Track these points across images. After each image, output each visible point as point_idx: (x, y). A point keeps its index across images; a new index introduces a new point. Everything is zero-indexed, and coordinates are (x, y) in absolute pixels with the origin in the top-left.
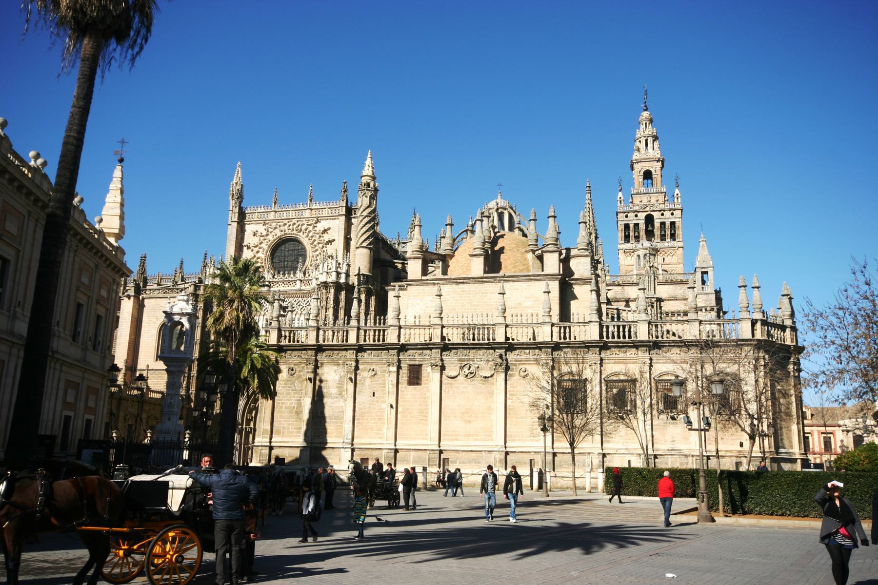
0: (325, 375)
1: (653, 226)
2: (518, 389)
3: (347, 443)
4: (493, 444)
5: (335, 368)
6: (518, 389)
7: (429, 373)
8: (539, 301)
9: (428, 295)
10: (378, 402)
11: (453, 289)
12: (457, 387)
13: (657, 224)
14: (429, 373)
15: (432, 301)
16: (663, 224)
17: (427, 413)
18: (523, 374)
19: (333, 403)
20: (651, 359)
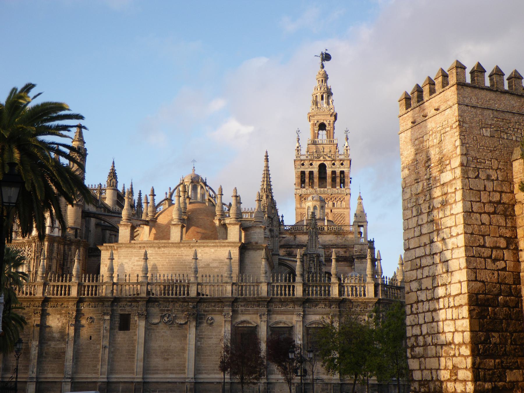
0: (50, 322)
1: (326, 173)
2: (206, 333)
3: (68, 378)
4: (186, 376)
5: (58, 316)
6: (206, 333)
7: (136, 321)
8: (223, 263)
9: (135, 256)
10: (94, 344)
11: (155, 251)
12: (158, 332)
13: (329, 171)
14: (136, 321)
15: (137, 261)
16: (334, 173)
17: (134, 353)
18: (209, 322)
19: (55, 345)
20: (304, 311)
